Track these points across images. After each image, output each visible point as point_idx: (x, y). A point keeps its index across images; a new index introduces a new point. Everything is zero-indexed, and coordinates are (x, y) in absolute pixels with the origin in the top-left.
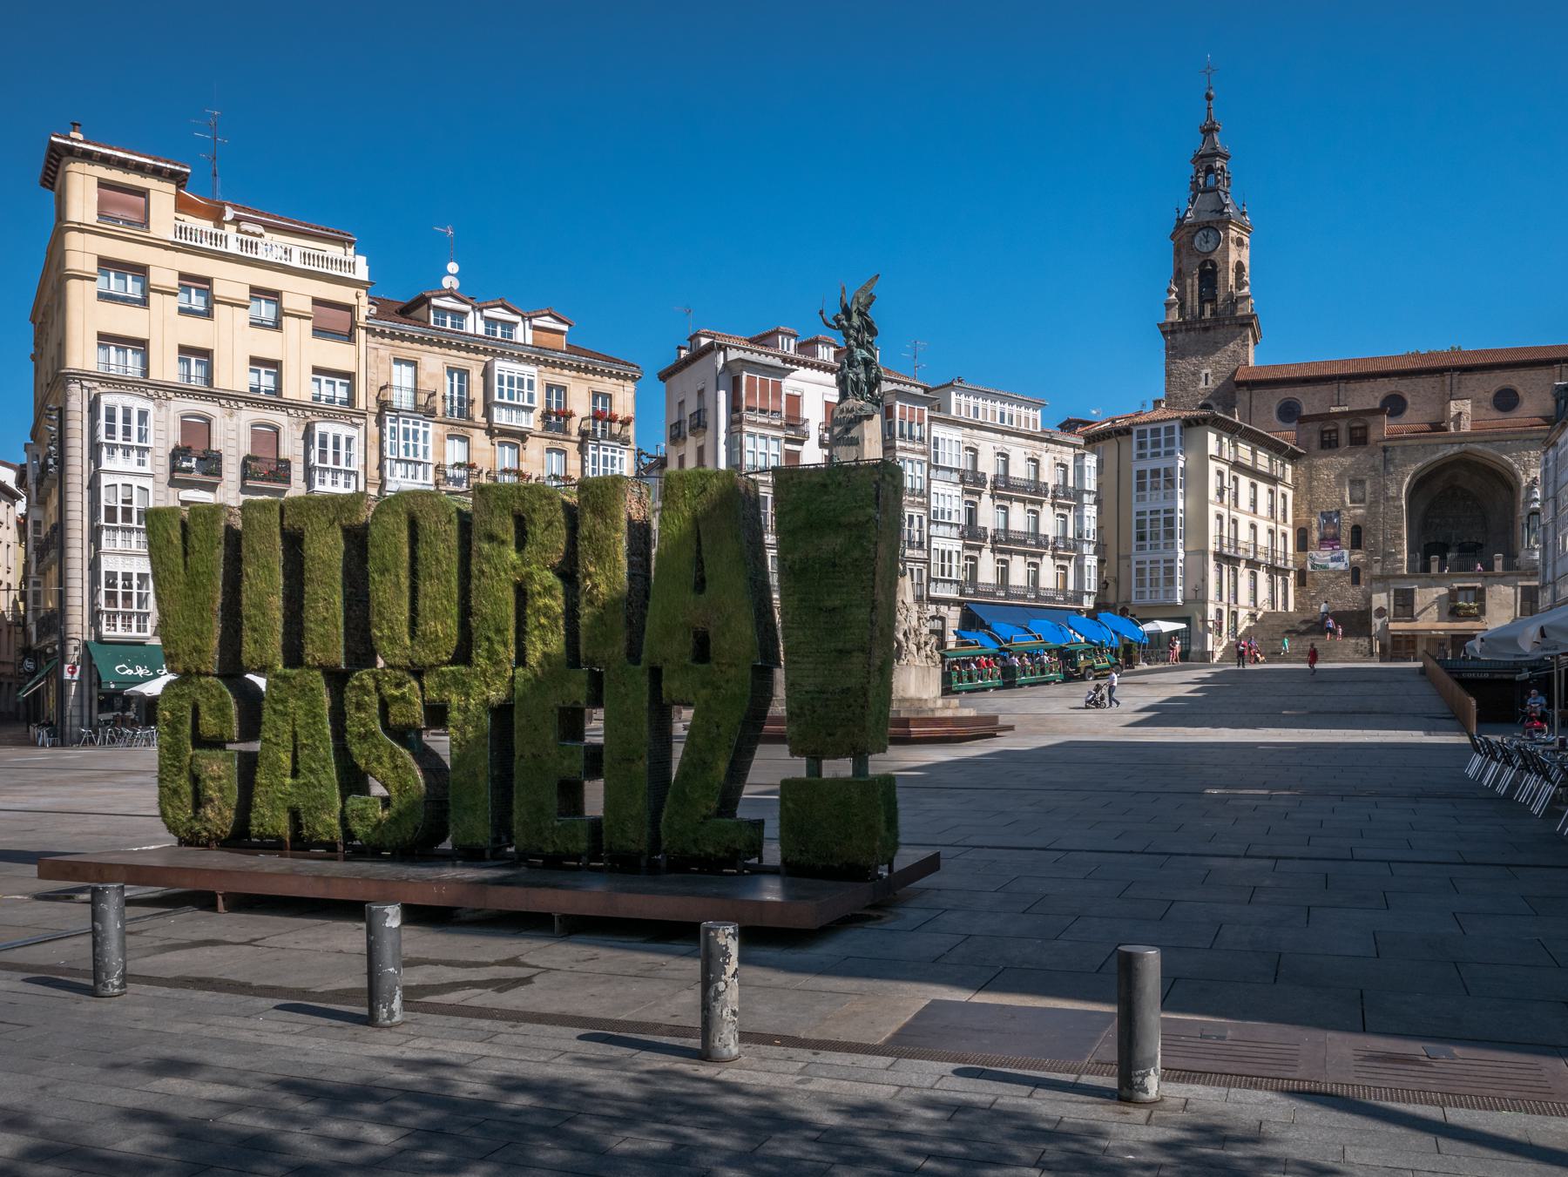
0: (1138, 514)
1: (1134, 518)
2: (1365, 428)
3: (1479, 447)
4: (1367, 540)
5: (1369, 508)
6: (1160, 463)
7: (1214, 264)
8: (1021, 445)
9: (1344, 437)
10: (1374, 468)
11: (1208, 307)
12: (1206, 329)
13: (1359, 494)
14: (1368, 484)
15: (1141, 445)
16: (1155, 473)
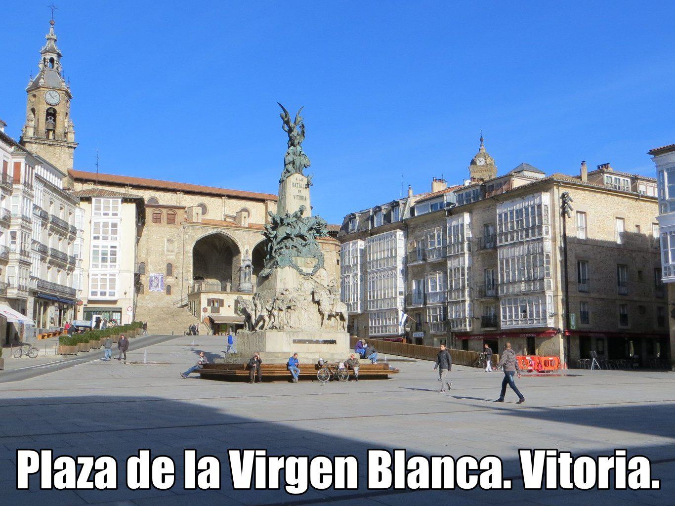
0: (95, 246)
1: (92, 249)
2: (174, 214)
3: (224, 231)
4: (175, 272)
5: (176, 256)
6: (111, 220)
7: (55, 111)
8: (58, 199)
9: (164, 217)
10: (179, 236)
11: (51, 133)
12: (50, 145)
13: (171, 248)
14: (176, 243)
15: (98, 208)
16: (105, 225)
